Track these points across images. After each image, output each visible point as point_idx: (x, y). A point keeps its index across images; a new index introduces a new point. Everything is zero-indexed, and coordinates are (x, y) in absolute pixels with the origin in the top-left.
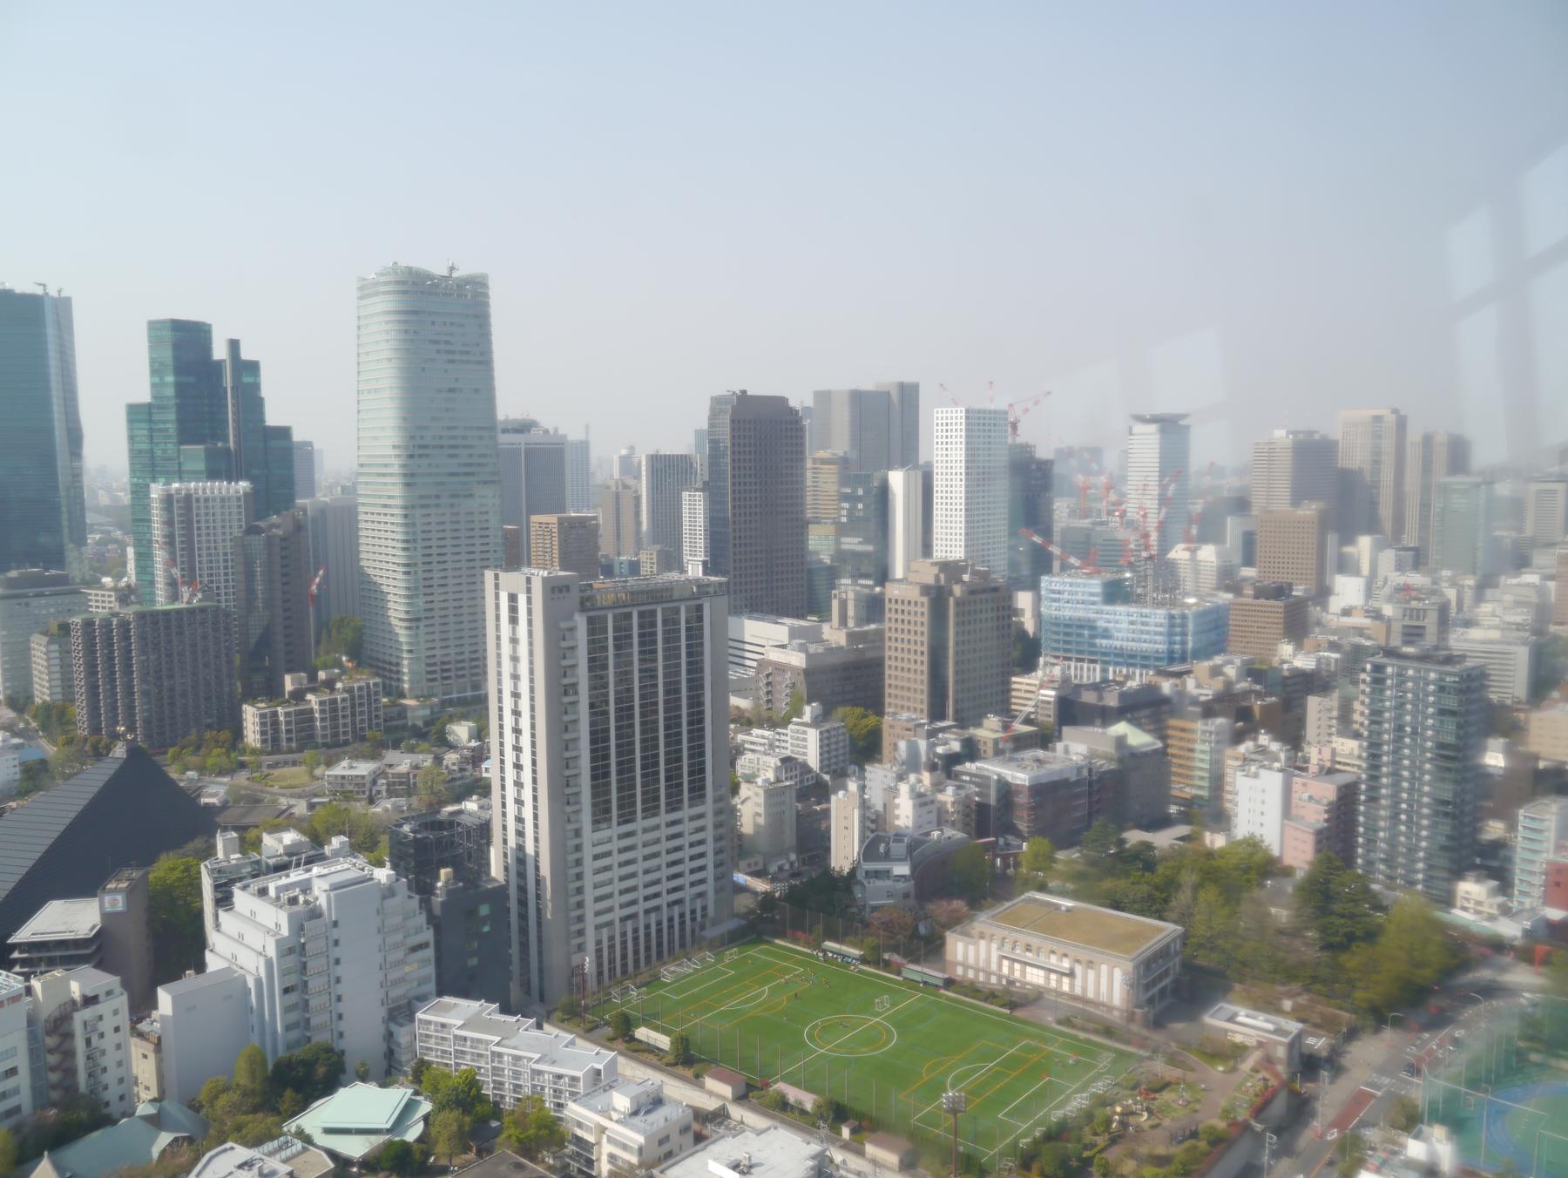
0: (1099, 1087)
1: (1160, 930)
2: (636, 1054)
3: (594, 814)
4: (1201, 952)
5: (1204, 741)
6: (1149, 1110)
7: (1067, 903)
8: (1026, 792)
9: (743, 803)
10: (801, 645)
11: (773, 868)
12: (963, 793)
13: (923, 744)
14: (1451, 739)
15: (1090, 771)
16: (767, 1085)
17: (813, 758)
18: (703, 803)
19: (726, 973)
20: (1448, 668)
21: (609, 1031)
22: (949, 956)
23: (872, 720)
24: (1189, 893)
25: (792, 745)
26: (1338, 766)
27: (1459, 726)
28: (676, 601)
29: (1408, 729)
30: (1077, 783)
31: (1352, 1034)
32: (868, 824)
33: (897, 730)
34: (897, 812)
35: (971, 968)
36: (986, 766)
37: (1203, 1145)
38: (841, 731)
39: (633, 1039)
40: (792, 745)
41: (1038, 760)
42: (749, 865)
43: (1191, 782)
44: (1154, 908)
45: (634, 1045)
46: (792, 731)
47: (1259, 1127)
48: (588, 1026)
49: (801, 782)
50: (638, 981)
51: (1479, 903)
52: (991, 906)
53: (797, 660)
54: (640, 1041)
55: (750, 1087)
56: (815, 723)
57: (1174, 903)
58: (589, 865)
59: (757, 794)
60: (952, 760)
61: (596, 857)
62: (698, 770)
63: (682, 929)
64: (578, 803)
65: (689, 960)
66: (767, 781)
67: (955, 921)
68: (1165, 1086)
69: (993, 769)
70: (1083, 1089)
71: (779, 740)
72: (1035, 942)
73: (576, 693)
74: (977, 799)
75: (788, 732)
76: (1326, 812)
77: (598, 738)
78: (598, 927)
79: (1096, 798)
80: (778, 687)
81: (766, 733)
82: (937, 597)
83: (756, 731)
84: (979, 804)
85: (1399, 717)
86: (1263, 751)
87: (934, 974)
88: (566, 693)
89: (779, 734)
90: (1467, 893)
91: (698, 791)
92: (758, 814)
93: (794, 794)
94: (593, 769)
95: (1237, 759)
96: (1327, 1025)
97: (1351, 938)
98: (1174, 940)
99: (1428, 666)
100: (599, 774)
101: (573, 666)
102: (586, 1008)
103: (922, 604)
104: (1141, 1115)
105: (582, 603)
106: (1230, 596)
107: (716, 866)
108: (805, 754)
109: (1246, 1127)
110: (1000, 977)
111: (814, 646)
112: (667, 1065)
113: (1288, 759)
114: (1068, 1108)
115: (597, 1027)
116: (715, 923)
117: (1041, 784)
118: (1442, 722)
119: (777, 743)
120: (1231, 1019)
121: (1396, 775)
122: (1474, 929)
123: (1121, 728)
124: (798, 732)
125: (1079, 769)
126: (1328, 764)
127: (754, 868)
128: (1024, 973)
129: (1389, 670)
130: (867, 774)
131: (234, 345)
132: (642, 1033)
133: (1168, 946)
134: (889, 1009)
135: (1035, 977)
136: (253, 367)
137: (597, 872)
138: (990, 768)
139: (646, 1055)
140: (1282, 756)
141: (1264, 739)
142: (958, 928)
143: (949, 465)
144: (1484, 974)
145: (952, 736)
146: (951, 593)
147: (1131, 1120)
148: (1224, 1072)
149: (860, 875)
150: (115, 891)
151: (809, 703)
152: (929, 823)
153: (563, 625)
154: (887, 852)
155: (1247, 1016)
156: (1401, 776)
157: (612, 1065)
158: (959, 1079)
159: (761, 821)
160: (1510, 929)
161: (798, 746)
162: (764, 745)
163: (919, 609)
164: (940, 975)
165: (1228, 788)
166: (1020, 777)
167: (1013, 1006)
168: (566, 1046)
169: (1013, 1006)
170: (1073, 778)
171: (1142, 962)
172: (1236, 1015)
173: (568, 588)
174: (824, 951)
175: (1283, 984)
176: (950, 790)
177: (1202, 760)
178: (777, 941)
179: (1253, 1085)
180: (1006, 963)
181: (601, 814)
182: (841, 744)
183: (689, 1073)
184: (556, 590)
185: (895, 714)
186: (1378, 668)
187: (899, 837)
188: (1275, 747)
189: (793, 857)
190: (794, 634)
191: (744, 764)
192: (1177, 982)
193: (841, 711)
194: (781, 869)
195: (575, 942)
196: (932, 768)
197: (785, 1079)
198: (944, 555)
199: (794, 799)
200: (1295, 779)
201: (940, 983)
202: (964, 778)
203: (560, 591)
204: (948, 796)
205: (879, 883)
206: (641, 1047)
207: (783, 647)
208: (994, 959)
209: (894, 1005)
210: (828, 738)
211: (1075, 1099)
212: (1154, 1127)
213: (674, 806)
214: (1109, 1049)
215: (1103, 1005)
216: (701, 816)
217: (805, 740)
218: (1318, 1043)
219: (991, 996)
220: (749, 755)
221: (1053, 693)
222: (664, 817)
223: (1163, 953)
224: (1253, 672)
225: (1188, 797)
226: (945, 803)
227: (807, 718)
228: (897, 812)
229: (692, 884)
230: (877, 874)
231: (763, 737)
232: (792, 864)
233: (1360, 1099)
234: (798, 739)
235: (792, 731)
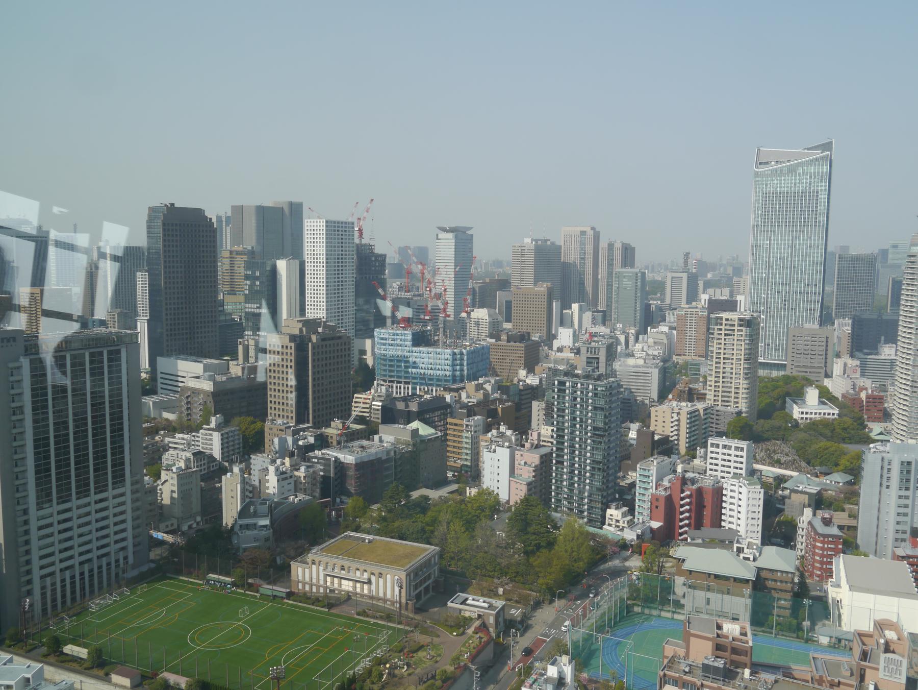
0: (379, 653)
1: (426, 550)
2: (63, 664)
3: (38, 497)
4: (453, 562)
5: (467, 431)
6: (408, 665)
7: (368, 537)
8: (353, 466)
9: (162, 484)
10: (211, 375)
11: (185, 528)
12: (311, 470)
13: (290, 440)
14: (601, 425)
15: (395, 452)
16: (157, 675)
17: (217, 453)
18: (124, 486)
19: (137, 601)
20: (599, 382)
21: (44, 650)
22: (293, 577)
23: (259, 424)
24: (445, 525)
25: (203, 443)
26: (541, 443)
27: (605, 417)
28: (101, 347)
29: (578, 419)
30: (387, 461)
31: (537, 605)
32: (247, 493)
33: (274, 431)
34: (267, 485)
35: (308, 584)
36: (328, 452)
37: (439, 683)
38: (236, 433)
39: (62, 653)
40: (203, 443)
41: (362, 447)
42: (167, 526)
43: (460, 457)
44: (424, 536)
45: (62, 658)
46: (202, 434)
47: (473, 667)
48: (29, 647)
49: (209, 468)
50: (71, 613)
51: (617, 521)
52: (320, 544)
53: (208, 386)
54: (67, 655)
55: (144, 677)
56: (218, 428)
57: (436, 533)
58: (34, 534)
59: (172, 478)
60: (310, 448)
61: (40, 528)
62: (119, 464)
63: (109, 574)
64: (26, 490)
65: (111, 595)
66: (179, 468)
67: (300, 553)
68: (421, 648)
69: (332, 453)
70: (367, 656)
71: (194, 441)
72: (346, 564)
73: (22, 413)
74: (322, 473)
75: (199, 435)
76: (534, 471)
77: (41, 444)
78: (42, 577)
79: (399, 469)
80: (195, 405)
81: (185, 436)
82: (300, 343)
83: (178, 435)
84: (323, 477)
85: (573, 412)
86: (502, 435)
87: (280, 590)
88: (14, 414)
89: (194, 436)
90: (611, 515)
91: (119, 478)
92: (173, 492)
93: (199, 477)
94: (36, 466)
95: (486, 441)
96: (522, 600)
97: (538, 547)
98: (434, 556)
99: (589, 381)
100: (42, 471)
101: (20, 394)
102: (28, 636)
103: (291, 348)
104: (403, 668)
105: (26, 350)
106: (493, 341)
107: (134, 528)
108: (211, 449)
109: (466, 667)
110: (326, 588)
111: (220, 376)
112: (86, 669)
113: (516, 440)
114: (357, 669)
115: (36, 648)
116: (134, 567)
117: (363, 462)
118: (596, 415)
119: (193, 443)
120: (464, 602)
121: (572, 446)
122: (610, 536)
123: (416, 424)
124: (206, 434)
125: (388, 452)
126: (536, 442)
127: (170, 528)
128: (340, 585)
129: (567, 384)
130: (252, 461)
132: (69, 649)
133: (430, 560)
134: (248, 616)
135: (347, 586)
137: (41, 538)
138: (331, 453)
139: (71, 664)
140: (513, 438)
141: (503, 428)
142: (299, 559)
143: (315, 257)
144: (616, 563)
145: (310, 434)
146: (310, 340)
147: (397, 672)
148: (457, 635)
149: (237, 528)
151: (215, 415)
152: (290, 490)
153: (11, 365)
154: (255, 512)
155: (473, 600)
156: (575, 447)
157: (39, 674)
158: (289, 657)
159: (175, 495)
160: (630, 535)
161: (206, 444)
162: (184, 444)
163: (289, 351)
164: (284, 590)
165: (481, 459)
166: (348, 458)
167: (330, 606)
168: (5, 664)
169: (330, 606)
170: (384, 457)
171: (412, 571)
172: (467, 599)
173: (14, 339)
174: (208, 581)
175: (499, 578)
176: (303, 469)
177: (466, 443)
178: (181, 578)
179: (474, 642)
180: (329, 579)
181: (44, 497)
182: (237, 442)
183: (101, 673)
184: (5, 340)
185: (273, 420)
186: (562, 383)
187: (264, 502)
188: (509, 433)
189: (199, 519)
190: (206, 368)
191: (167, 458)
192: (436, 582)
193: (237, 420)
194: (190, 527)
195: (24, 589)
196: (292, 455)
197: (169, 670)
198: (313, 315)
200: (517, 452)
201: (284, 595)
202: (314, 460)
203: (8, 341)
204: (301, 473)
205: (248, 533)
206: (68, 658)
207: (198, 377)
208: (321, 577)
209: (251, 613)
210: (227, 438)
211: (363, 662)
212: (410, 675)
214: (390, 628)
215: (379, 599)
216: (122, 495)
217: (211, 440)
218: (516, 613)
219: (316, 601)
220: (171, 452)
221: (380, 404)
222: (93, 497)
223: (427, 564)
224: (499, 387)
225: (459, 466)
226: (300, 477)
227: (213, 425)
228: (267, 485)
229: (116, 542)
230: (248, 527)
231: (183, 439)
232: (198, 524)
233: (538, 643)
234: (206, 439)
235: (202, 434)
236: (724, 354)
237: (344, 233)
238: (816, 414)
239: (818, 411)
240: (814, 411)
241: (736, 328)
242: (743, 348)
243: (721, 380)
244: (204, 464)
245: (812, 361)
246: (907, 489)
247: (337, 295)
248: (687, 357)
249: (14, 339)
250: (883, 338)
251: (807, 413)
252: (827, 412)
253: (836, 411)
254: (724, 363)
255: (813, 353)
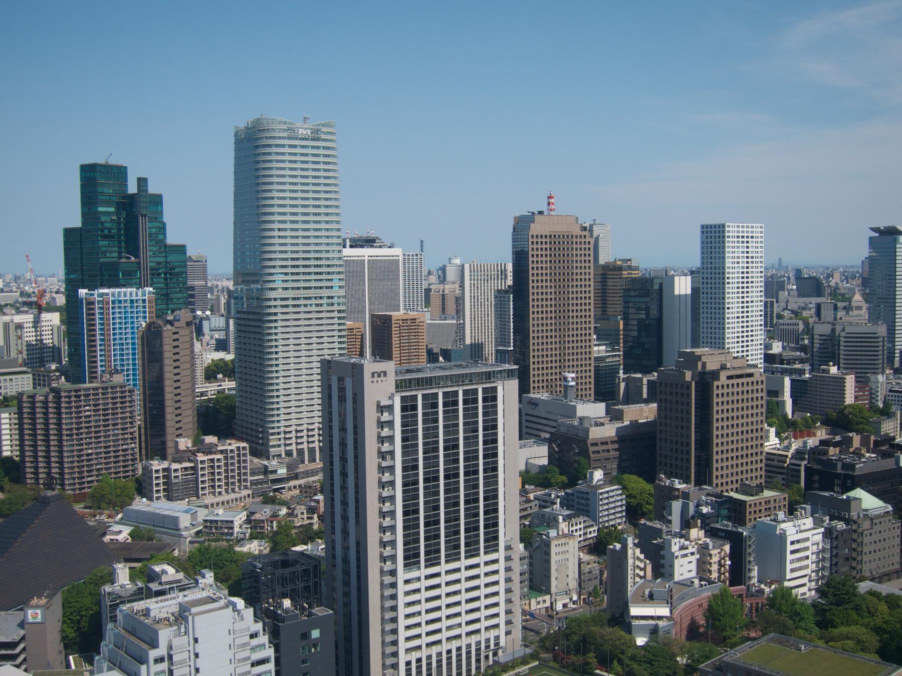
18: (497, 551)
32: (637, 571)
49: (585, 534)
123: (859, 493)
131: (142, 182)
136: (158, 200)
150: (37, 607)
181: (411, 559)
184: (376, 375)
199: (577, 549)
203: (379, 376)
213: (472, 552)
216: (496, 561)
237: (750, 240)
244: (580, 529)
247: (740, 320)
249: (385, 374)
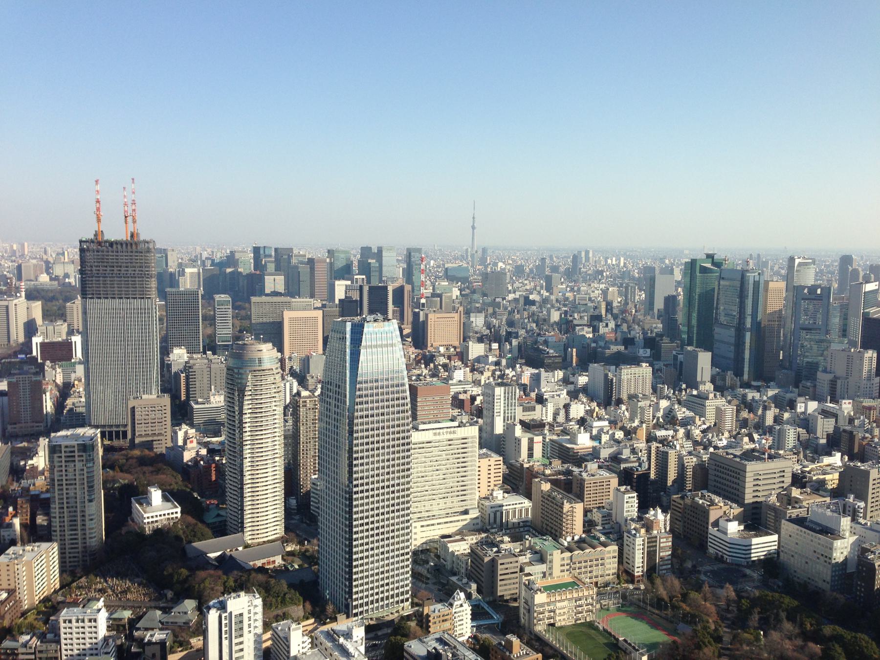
236: (66, 480)
238: (160, 515)
239: (162, 513)
240: (158, 513)
241: (76, 454)
242: (85, 472)
243: (65, 505)
245: (152, 428)
246: (241, 636)
248: (23, 425)
250: (213, 387)
251: (152, 517)
252: (170, 511)
253: (179, 510)
254: (67, 489)
255: (154, 421)
